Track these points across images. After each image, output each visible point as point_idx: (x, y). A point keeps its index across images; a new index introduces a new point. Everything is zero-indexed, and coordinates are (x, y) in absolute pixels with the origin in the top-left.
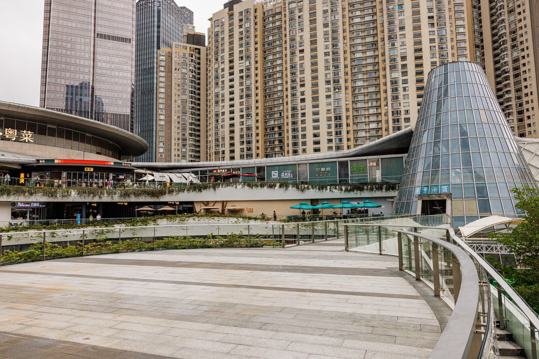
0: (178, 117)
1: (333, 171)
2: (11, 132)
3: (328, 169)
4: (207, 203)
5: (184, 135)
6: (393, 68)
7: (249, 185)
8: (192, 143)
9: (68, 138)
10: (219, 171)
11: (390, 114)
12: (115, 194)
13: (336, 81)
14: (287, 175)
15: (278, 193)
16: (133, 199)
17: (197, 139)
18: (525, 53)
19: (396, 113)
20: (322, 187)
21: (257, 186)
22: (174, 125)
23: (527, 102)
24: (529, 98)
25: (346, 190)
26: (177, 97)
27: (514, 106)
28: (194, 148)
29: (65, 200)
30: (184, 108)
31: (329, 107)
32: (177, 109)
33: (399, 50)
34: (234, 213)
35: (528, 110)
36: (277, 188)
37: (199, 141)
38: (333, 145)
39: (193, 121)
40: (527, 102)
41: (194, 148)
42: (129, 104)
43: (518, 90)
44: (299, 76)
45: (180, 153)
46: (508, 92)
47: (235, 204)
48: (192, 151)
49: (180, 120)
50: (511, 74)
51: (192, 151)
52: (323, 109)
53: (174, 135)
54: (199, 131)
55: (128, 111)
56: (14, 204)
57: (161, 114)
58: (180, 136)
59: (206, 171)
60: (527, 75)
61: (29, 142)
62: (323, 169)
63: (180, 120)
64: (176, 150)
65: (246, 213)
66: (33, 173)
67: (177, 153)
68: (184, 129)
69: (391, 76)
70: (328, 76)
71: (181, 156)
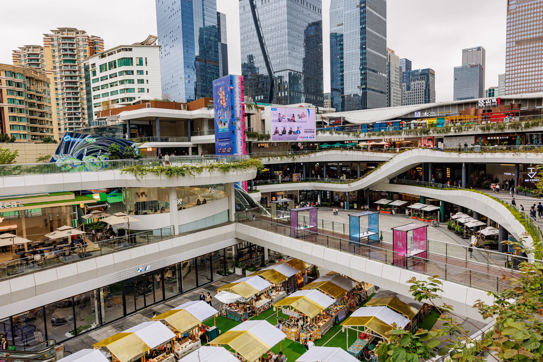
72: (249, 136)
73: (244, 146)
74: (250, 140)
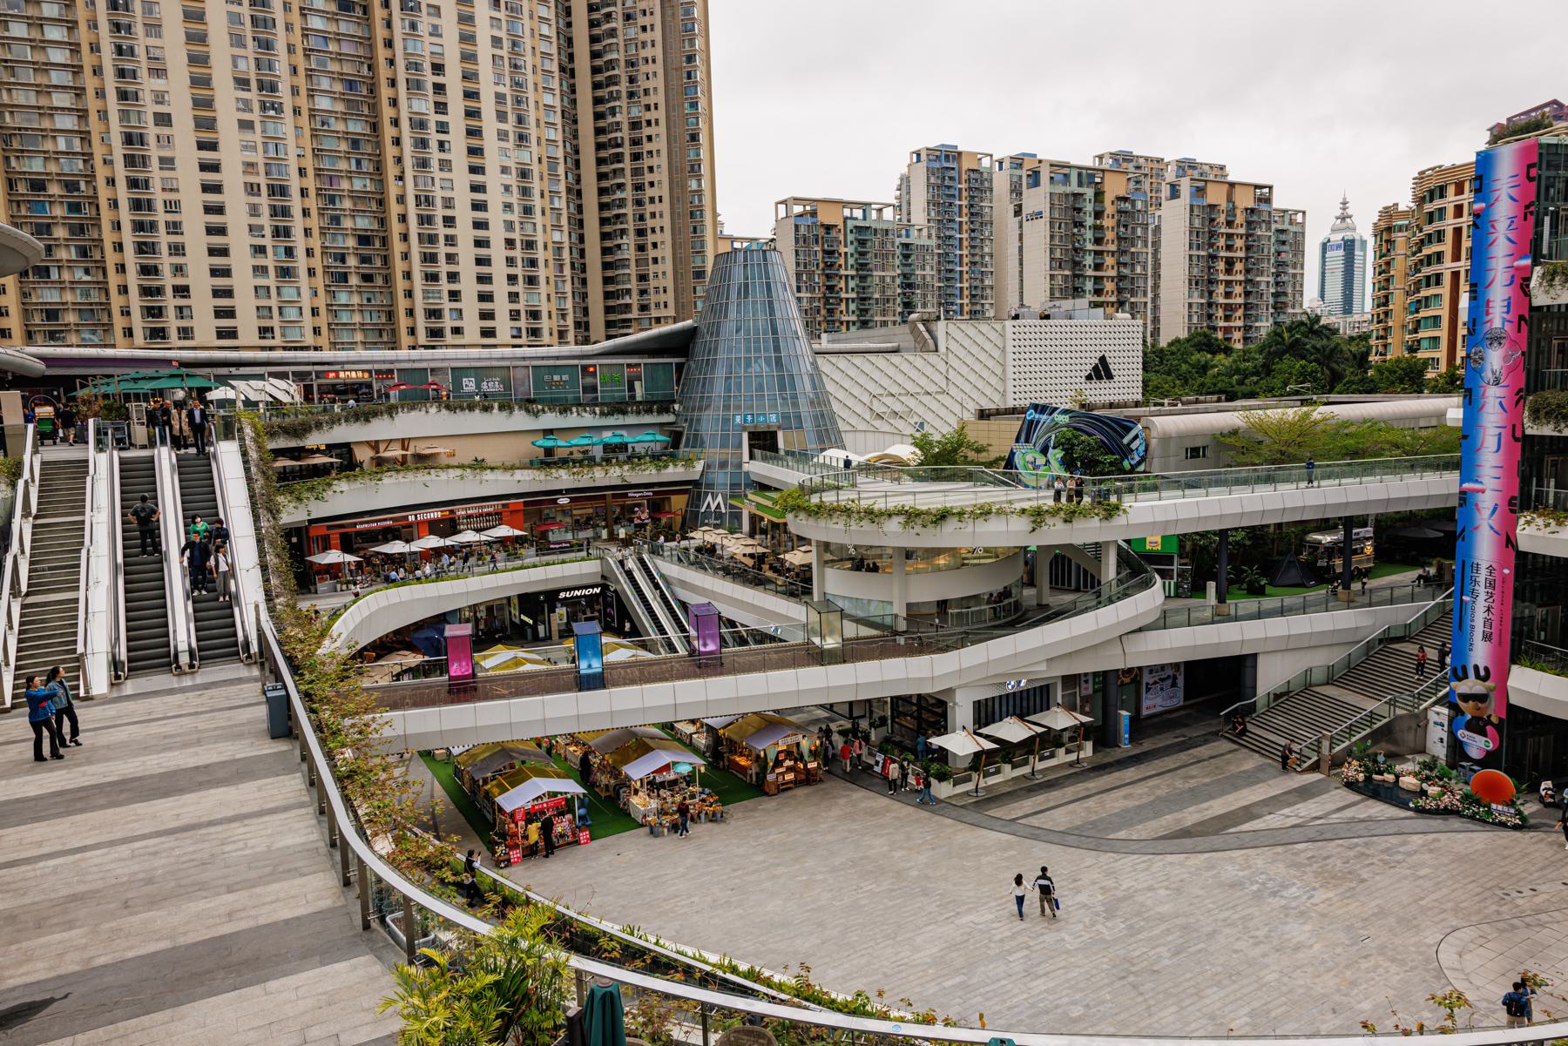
1: (573, 381)
3: (565, 377)
4: (374, 445)
6: (415, 86)
7: (448, 407)
10: (342, 375)
11: (411, 201)
13: (268, 87)
14: (492, 386)
15: (497, 421)
18: (652, 115)
19: (425, 200)
20: (565, 410)
21: (462, 409)
23: (653, 215)
24: (656, 207)
25: (602, 414)
27: (630, 218)
31: (250, 157)
33: (427, 44)
34: (424, 461)
35: (653, 231)
36: (495, 411)
38: (269, 261)
40: (653, 215)
43: (638, 187)
44: (141, 41)
46: (620, 186)
47: (435, 443)
50: (626, 150)
52: (231, 154)
59: (309, 373)
60: (654, 162)
62: (556, 378)
65: (444, 461)
69: (410, 107)
70: (242, 65)
72: (1536, 415)
73: (1509, 453)
74: (1547, 430)
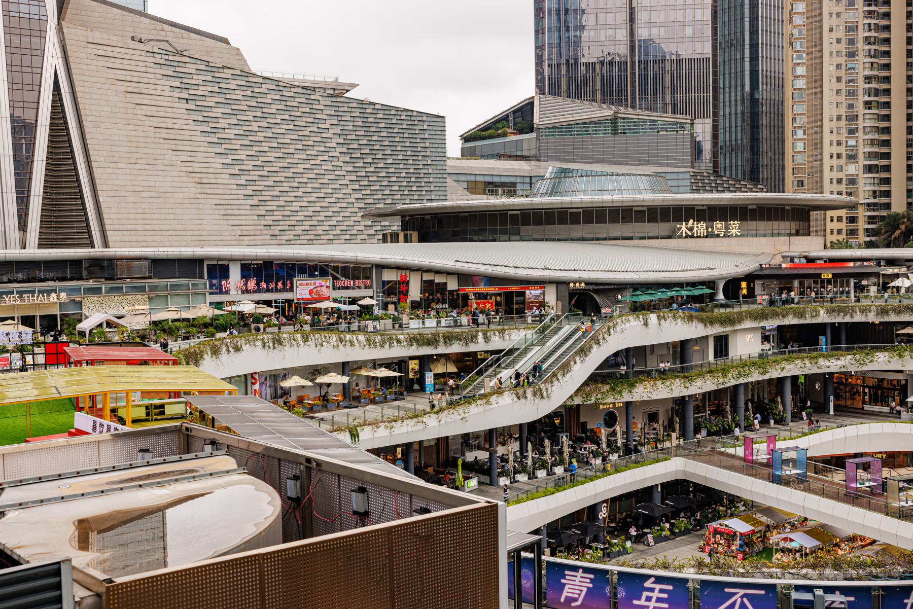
0: (839, 66)
2: (719, 226)
5: (851, 106)
8: (872, 124)
9: (769, 219)
12: (870, 312)
16: (893, 318)
17: (884, 112)
22: (829, 86)
26: (835, 21)
28: (876, 136)
29: (814, 321)
30: (852, 42)
32: (836, 47)
37: (888, 118)
39: (875, 73)
41: (876, 136)
42: (709, 32)
45: (842, 150)
48: (872, 142)
49: (842, 73)
51: (872, 142)
53: (829, 111)
54: (888, 92)
55: (704, 49)
56: (763, 328)
57: (798, 64)
58: (843, 111)
61: (737, 236)
63: (842, 73)
64: (835, 143)
66: (757, 282)
67: (835, 150)
68: (852, 93)
71: (844, 156)
